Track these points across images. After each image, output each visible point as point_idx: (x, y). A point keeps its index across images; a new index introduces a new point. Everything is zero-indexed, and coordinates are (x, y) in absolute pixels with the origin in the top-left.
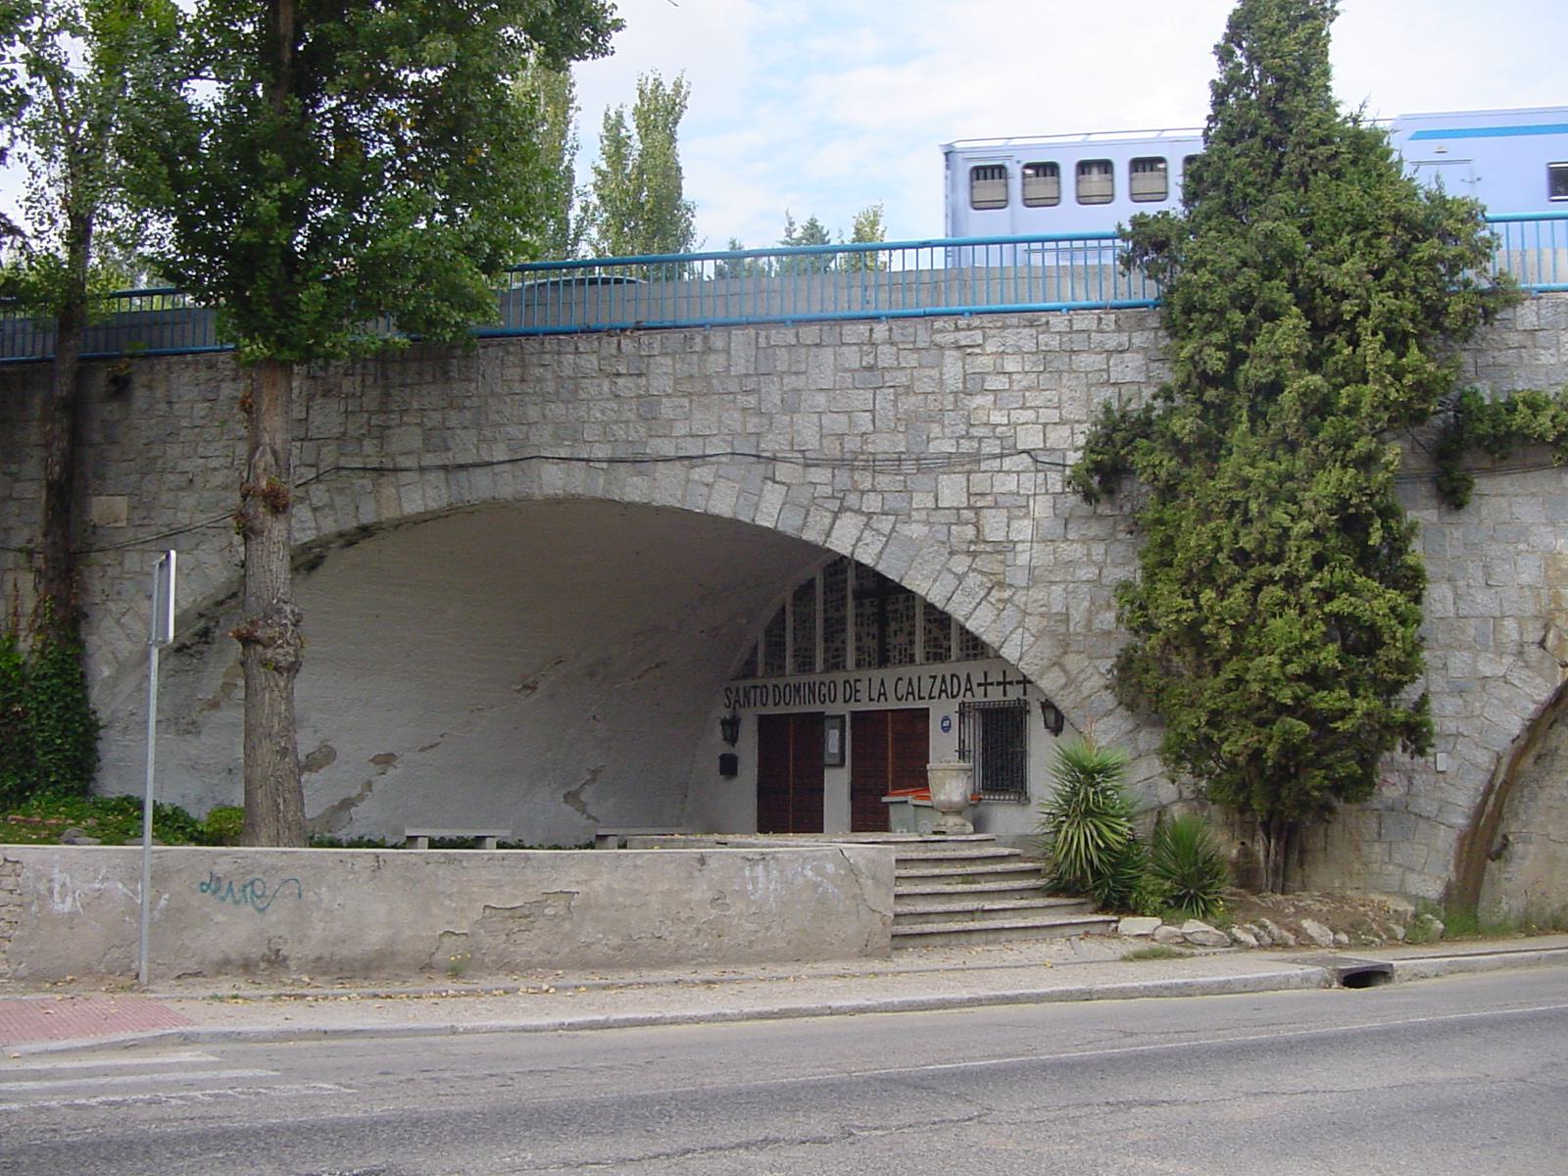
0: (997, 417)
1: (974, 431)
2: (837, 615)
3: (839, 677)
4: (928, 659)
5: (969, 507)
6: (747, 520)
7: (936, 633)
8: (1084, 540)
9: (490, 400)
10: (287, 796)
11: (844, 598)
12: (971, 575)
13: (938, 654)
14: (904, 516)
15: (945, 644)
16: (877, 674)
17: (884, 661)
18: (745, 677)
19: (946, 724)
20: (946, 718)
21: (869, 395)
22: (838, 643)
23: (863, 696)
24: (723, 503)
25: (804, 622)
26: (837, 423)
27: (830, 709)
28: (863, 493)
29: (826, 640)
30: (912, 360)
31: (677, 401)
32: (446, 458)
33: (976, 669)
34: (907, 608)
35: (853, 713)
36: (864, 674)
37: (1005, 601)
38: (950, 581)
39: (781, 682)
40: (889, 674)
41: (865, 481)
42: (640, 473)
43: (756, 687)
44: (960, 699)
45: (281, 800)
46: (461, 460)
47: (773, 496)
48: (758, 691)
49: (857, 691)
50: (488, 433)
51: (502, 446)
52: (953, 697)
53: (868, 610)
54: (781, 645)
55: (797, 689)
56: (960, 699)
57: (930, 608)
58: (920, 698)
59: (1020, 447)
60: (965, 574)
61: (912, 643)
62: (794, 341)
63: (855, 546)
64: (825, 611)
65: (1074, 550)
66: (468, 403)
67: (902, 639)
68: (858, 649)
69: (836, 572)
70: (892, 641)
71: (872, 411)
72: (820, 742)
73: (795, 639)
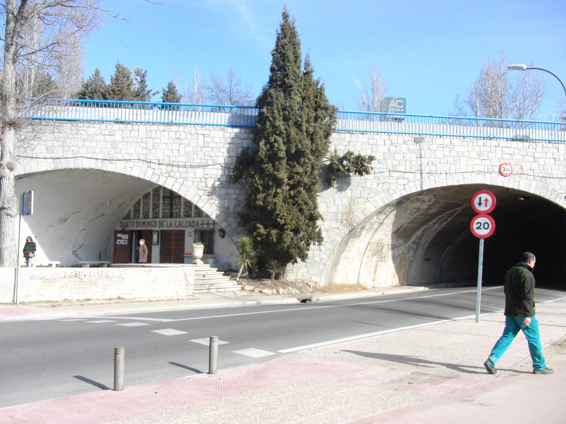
0: (212, 154)
1: (206, 158)
2: (157, 203)
3: (158, 220)
4: (185, 216)
5: (204, 178)
6: (143, 178)
7: (187, 209)
8: (234, 188)
9: (67, 140)
10: (14, 252)
11: (159, 198)
12: (204, 196)
13: (188, 215)
14: (185, 179)
15: (190, 212)
16: (169, 220)
17: (171, 216)
18: (127, 219)
19: (190, 234)
20: (190, 233)
21: (178, 145)
22: (157, 211)
23: (165, 226)
24: (136, 173)
25: (146, 204)
26: (169, 153)
27: (154, 229)
28: (175, 172)
29: (153, 209)
30: (189, 137)
31: (123, 144)
32: (54, 156)
33: (200, 220)
34: (179, 202)
35: (162, 231)
36: (165, 220)
37: (212, 203)
38: (198, 197)
39: (139, 221)
40: (173, 220)
41: (175, 169)
42: (112, 163)
43: (130, 222)
44: (195, 228)
45: (11, 254)
46: (58, 156)
47: (150, 171)
48: (131, 223)
49: (163, 224)
50: (66, 149)
51: (71, 153)
52: (193, 227)
53: (167, 202)
54: (139, 210)
55: (144, 223)
56: (195, 228)
57: (196, 207)
58: (183, 227)
59: (218, 162)
60: (202, 195)
61: (180, 212)
62: (157, 129)
63: (172, 186)
64: (153, 201)
65: (231, 191)
66: (60, 140)
67: (177, 211)
68: (163, 212)
69: (157, 191)
70: (174, 211)
71: (179, 150)
72: (152, 238)
73: (143, 209)
